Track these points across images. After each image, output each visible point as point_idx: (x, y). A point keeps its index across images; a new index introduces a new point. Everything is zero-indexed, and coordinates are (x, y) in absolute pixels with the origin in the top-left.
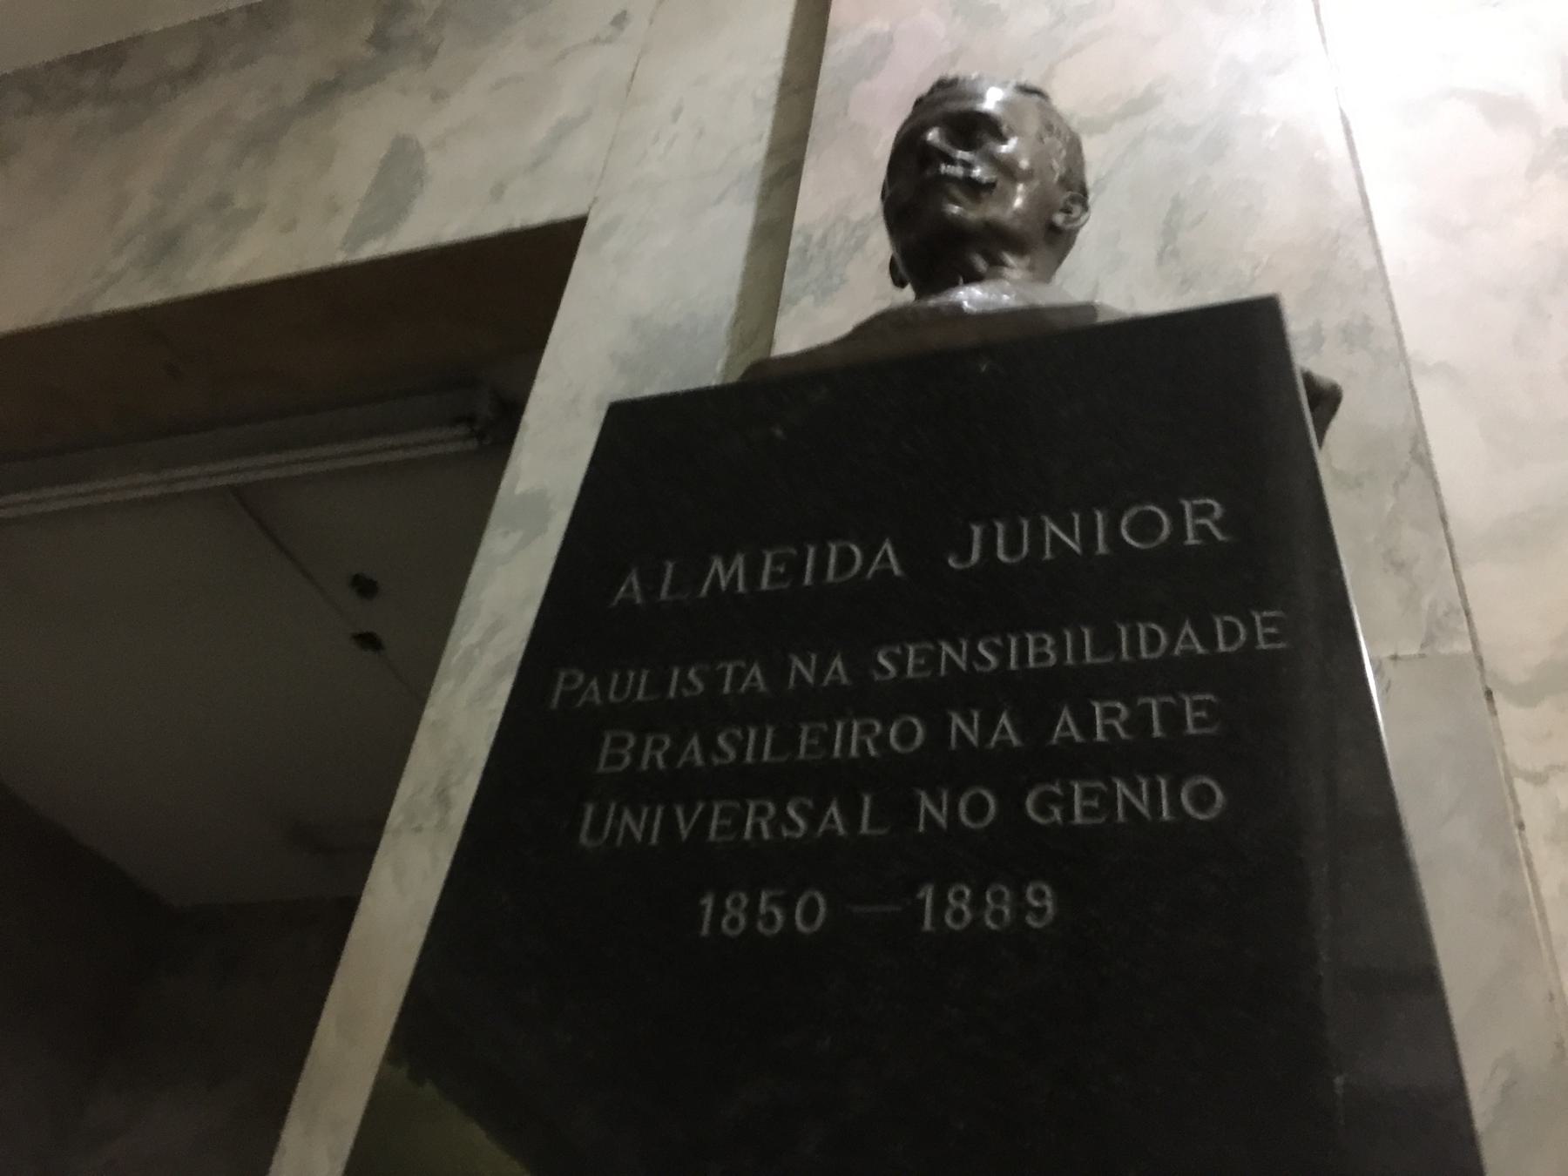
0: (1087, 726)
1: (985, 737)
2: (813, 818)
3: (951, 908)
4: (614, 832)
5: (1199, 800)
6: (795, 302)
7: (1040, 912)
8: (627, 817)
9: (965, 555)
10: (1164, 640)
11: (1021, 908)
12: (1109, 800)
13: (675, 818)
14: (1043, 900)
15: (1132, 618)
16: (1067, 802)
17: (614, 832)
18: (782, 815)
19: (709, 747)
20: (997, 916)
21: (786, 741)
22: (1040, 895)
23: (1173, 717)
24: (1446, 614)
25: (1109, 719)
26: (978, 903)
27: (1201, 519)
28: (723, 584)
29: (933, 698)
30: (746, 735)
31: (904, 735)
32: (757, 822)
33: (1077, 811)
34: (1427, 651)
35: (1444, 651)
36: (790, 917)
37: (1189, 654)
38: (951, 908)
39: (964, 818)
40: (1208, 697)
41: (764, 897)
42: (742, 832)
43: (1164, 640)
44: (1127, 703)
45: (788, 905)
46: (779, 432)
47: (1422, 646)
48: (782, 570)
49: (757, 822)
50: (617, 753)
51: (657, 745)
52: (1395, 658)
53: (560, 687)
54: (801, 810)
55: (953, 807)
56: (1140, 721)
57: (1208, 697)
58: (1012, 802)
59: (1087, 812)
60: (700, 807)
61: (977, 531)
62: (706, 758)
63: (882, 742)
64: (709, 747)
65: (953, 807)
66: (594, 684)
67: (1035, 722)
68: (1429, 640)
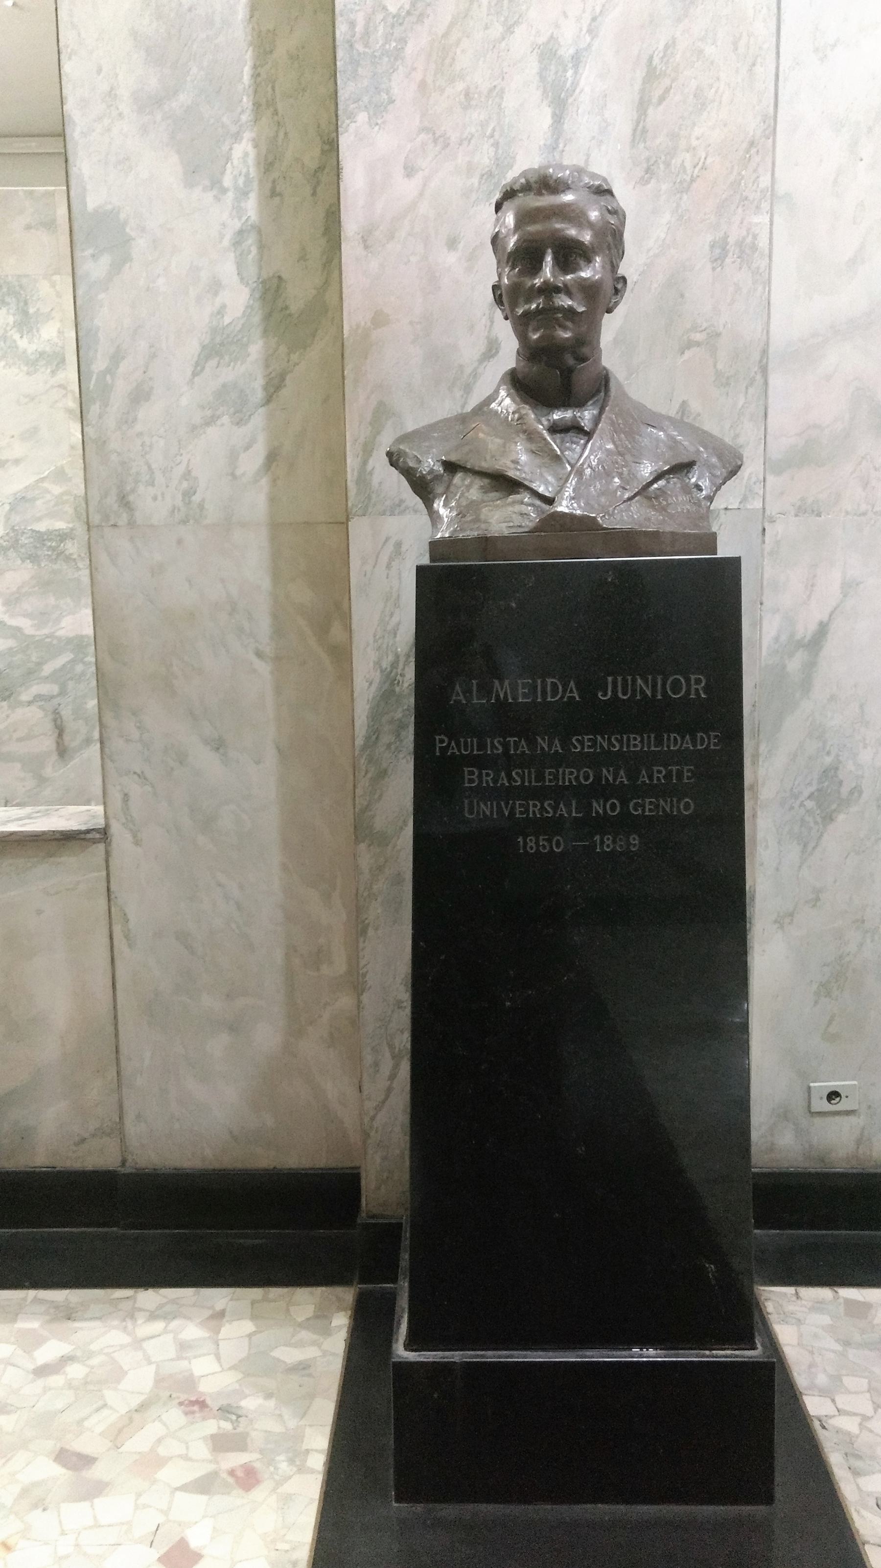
0: (651, 777)
1: (615, 780)
2: (555, 808)
3: (607, 844)
4: (478, 812)
5: (686, 807)
6: (351, 116)
7: (635, 845)
8: (482, 806)
9: (605, 695)
10: (679, 742)
11: (629, 844)
12: (657, 806)
13: (501, 807)
14: (635, 840)
15: (669, 731)
16: (643, 806)
17: (478, 812)
18: (542, 807)
19: (510, 778)
20: (621, 846)
21: (540, 777)
22: (634, 839)
23: (680, 774)
24: (755, 483)
25: (659, 773)
26: (614, 842)
27: (697, 686)
28: (502, 696)
29: (594, 761)
30: (524, 772)
31: (585, 776)
32: (534, 809)
33: (647, 810)
34: (741, 506)
35: (749, 507)
36: (551, 847)
37: (687, 749)
38: (607, 844)
39: (609, 811)
40: (692, 767)
41: (541, 838)
42: (528, 814)
43: (679, 742)
44: (666, 769)
45: (549, 841)
46: (514, 605)
47: (740, 503)
48: (526, 691)
49: (534, 809)
50: (471, 778)
51: (488, 775)
52: (726, 509)
53: (438, 745)
54: (549, 805)
55: (605, 806)
56: (668, 776)
57: (692, 767)
58: (624, 803)
59: (650, 810)
60: (511, 802)
61: (610, 679)
62: (509, 783)
63: (577, 778)
64: (510, 778)
65: (605, 806)
66: (453, 744)
67: (633, 775)
68: (744, 500)
